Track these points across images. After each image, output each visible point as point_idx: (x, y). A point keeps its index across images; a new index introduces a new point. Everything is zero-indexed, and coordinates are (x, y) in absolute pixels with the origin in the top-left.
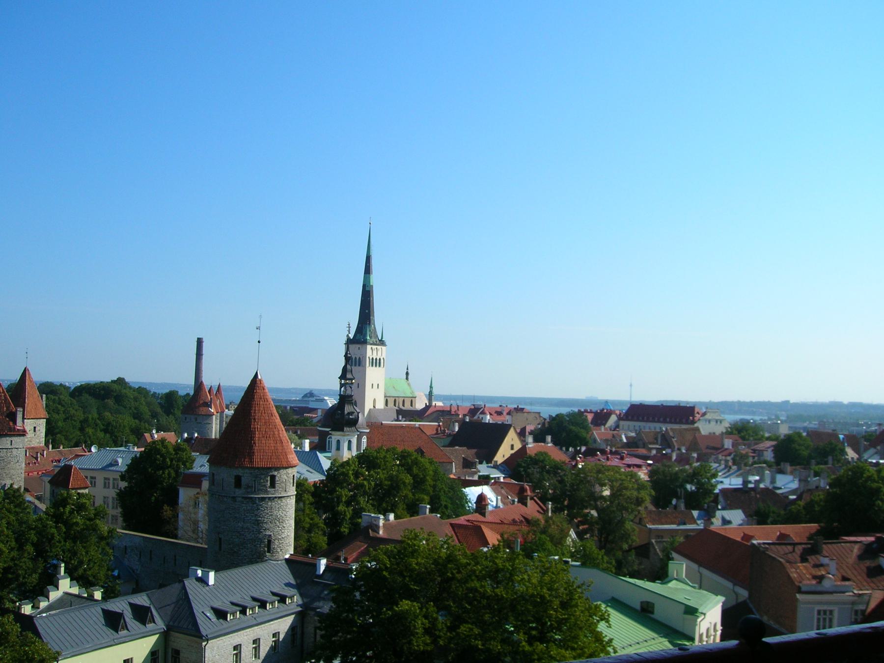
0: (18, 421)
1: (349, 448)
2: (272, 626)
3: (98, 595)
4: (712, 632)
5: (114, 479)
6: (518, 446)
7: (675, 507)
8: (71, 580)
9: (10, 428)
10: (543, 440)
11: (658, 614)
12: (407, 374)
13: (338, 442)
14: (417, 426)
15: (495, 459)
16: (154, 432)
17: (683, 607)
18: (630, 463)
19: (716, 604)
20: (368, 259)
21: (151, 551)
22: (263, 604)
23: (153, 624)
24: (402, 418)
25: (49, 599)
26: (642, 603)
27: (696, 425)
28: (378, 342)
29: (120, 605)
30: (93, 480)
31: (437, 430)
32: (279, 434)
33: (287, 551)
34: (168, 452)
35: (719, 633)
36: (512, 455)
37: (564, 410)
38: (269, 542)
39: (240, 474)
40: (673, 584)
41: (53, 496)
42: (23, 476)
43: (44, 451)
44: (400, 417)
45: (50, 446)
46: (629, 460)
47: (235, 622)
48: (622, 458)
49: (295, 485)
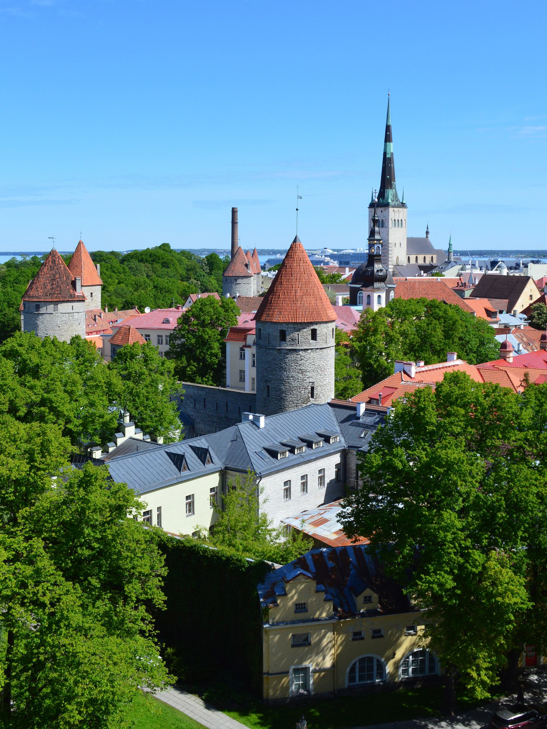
1: (379, 303)
2: (318, 463)
5: (166, 336)
6: (537, 295)
8: (136, 427)
9: (71, 295)
12: (427, 233)
14: (439, 280)
15: (515, 309)
21: (205, 399)
23: (211, 464)
24: (424, 273)
25: (116, 444)
30: (148, 338)
31: (458, 283)
33: (328, 396)
36: (531, 305)
38: (313, 388)
41: (114, 354)
44: (422, 272)
47: (285, 460)
49: (334, 335)
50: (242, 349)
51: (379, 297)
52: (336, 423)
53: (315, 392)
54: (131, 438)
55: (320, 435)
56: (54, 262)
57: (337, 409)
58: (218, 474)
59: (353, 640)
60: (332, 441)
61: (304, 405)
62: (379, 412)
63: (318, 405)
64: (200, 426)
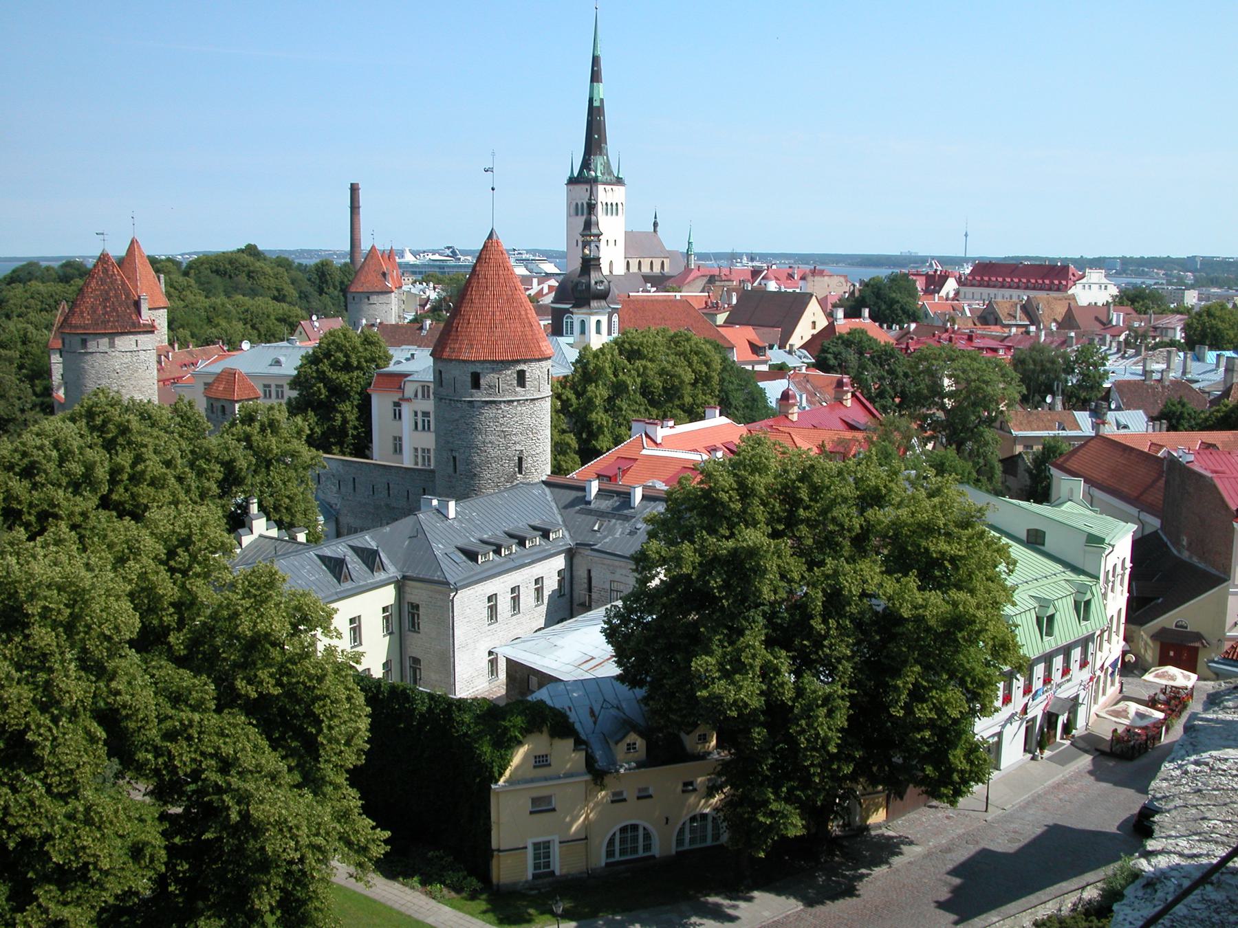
0: (143, 314)
1: (598, 332)
3: (302, 537)
4: (1119, 570)
5: (277, 386)
6: (822, 323)
7: (1051, 407)
10: (859, 315)
11: (1050, 545)
12: (655, 225)
13: (583, 322)
14: (678, 298)
15: (791, 342)
16: (314, 318)
17: (1084, 539)
18: (982, 346)
19: (1128, 531)
20: (596, 61)
22: (521, 542)
26: (1028, 531)
27: (1070, 292)
28: (614, 180)
29: (338, 549)
31: (706, 303)
32: (526, 314)
34: (354, 348)
35: (1128, 572)
36: (813, 336)
37: (883, 273)
38: (520, 459)
39: (479, 371)
40: (1065, 507)
41: (213, 412)
42: (156, 387)
43: (168, 352)
44: (649, 285)
45: (176, 346)
46: (978, 342)
47: (489, 565)
48: (970, 338)
50: (397, 404)
51: (598, 322)
52: (555, 510)
53: (524, 466)
54: (261, 536)
55: (535, 528)
56: (106, 271)
57: (557, 490)
58: (392, 586)
59: (613, 802)
60: (552, 536)
61: (509, 485)
62: (618, 493)
63: (528, 484)
64: (346, 520)
